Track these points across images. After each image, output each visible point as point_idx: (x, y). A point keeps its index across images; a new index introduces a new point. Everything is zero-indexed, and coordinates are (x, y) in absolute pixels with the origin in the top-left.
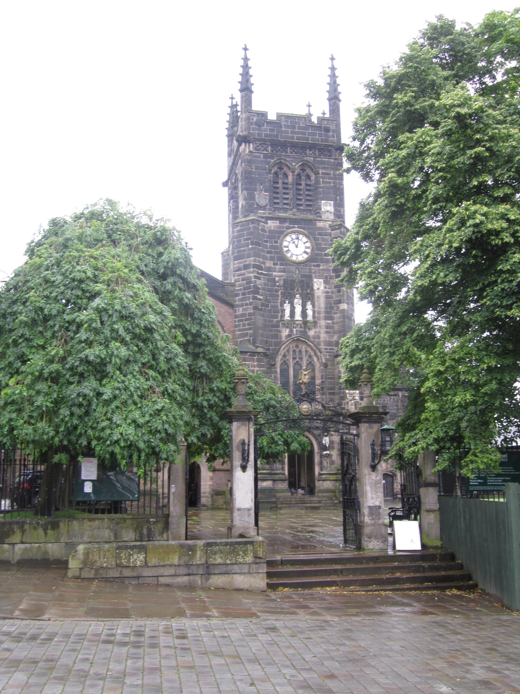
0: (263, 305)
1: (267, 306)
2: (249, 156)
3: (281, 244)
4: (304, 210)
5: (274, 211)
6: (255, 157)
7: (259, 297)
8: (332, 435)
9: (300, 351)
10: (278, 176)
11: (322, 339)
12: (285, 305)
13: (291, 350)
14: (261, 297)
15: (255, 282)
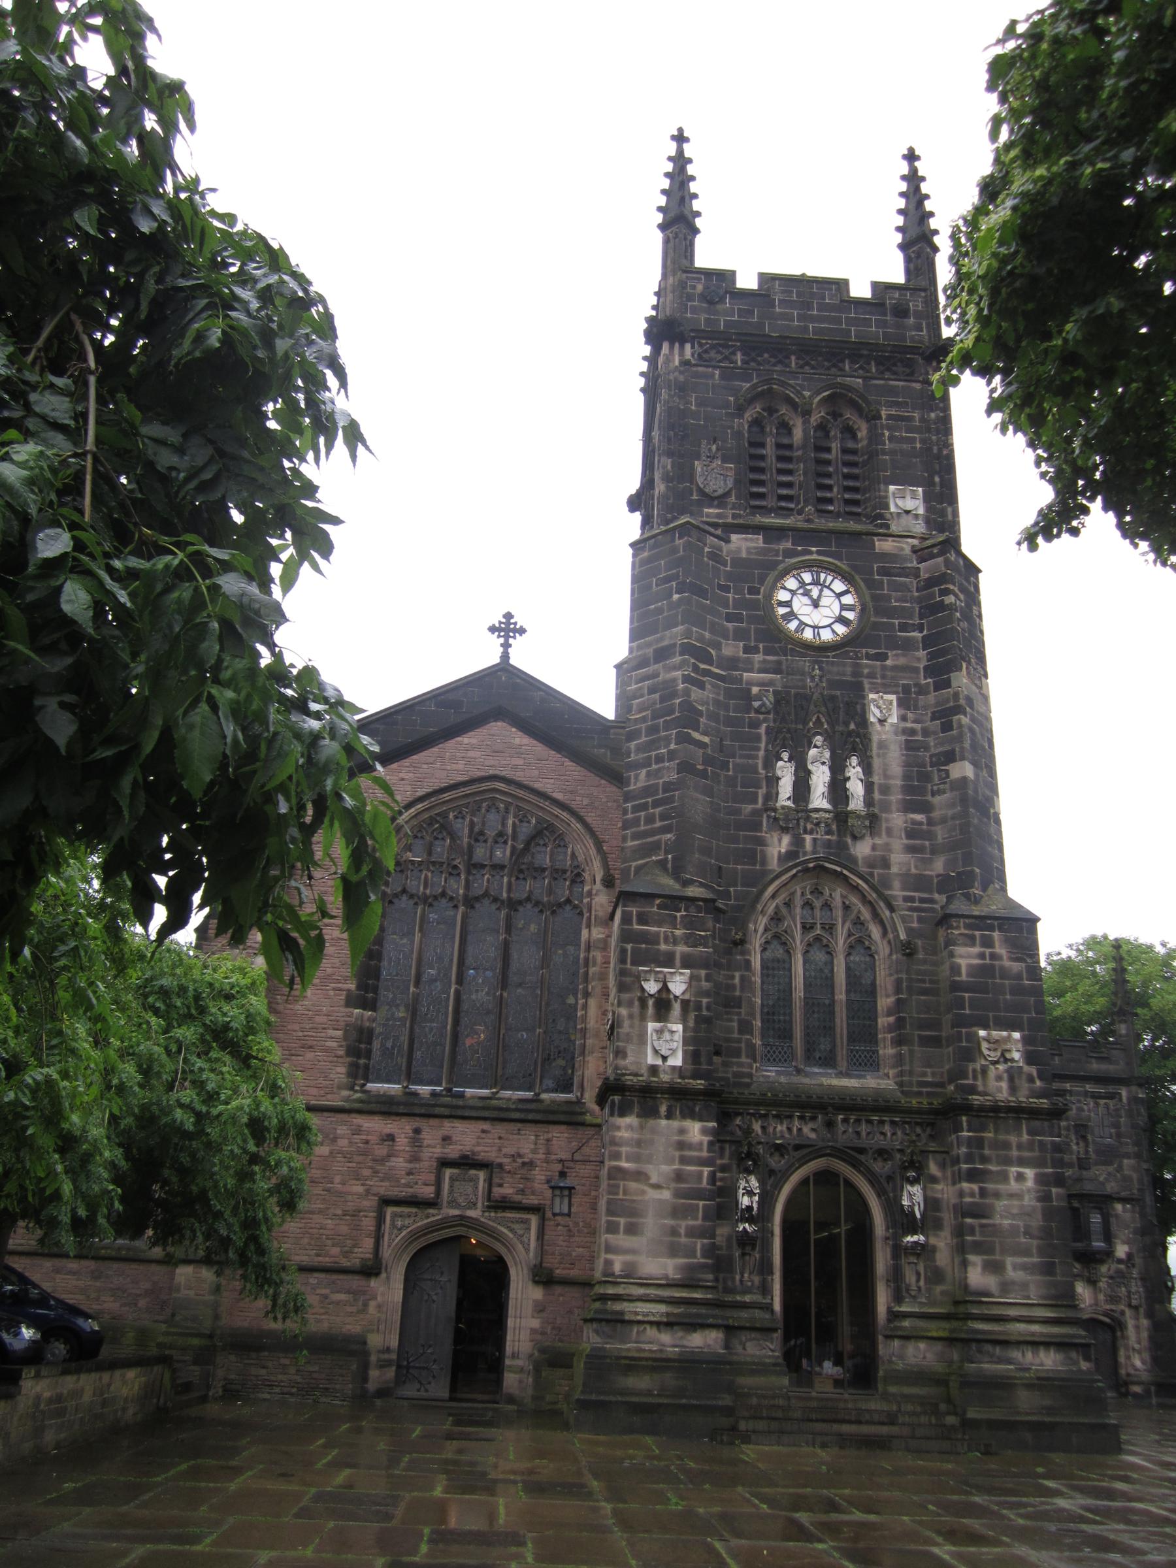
0: (708, 761)
1: (725, 766)
2: (681, 373)
3: (770, 596)
5: (753, 514)
6: (697, 375)
8: (934, 1180)
9: (827, 906)
11: (894, 870)
12: (780, 764)
13: (798, 901)
14: (706, 739)
15: (687, 692)
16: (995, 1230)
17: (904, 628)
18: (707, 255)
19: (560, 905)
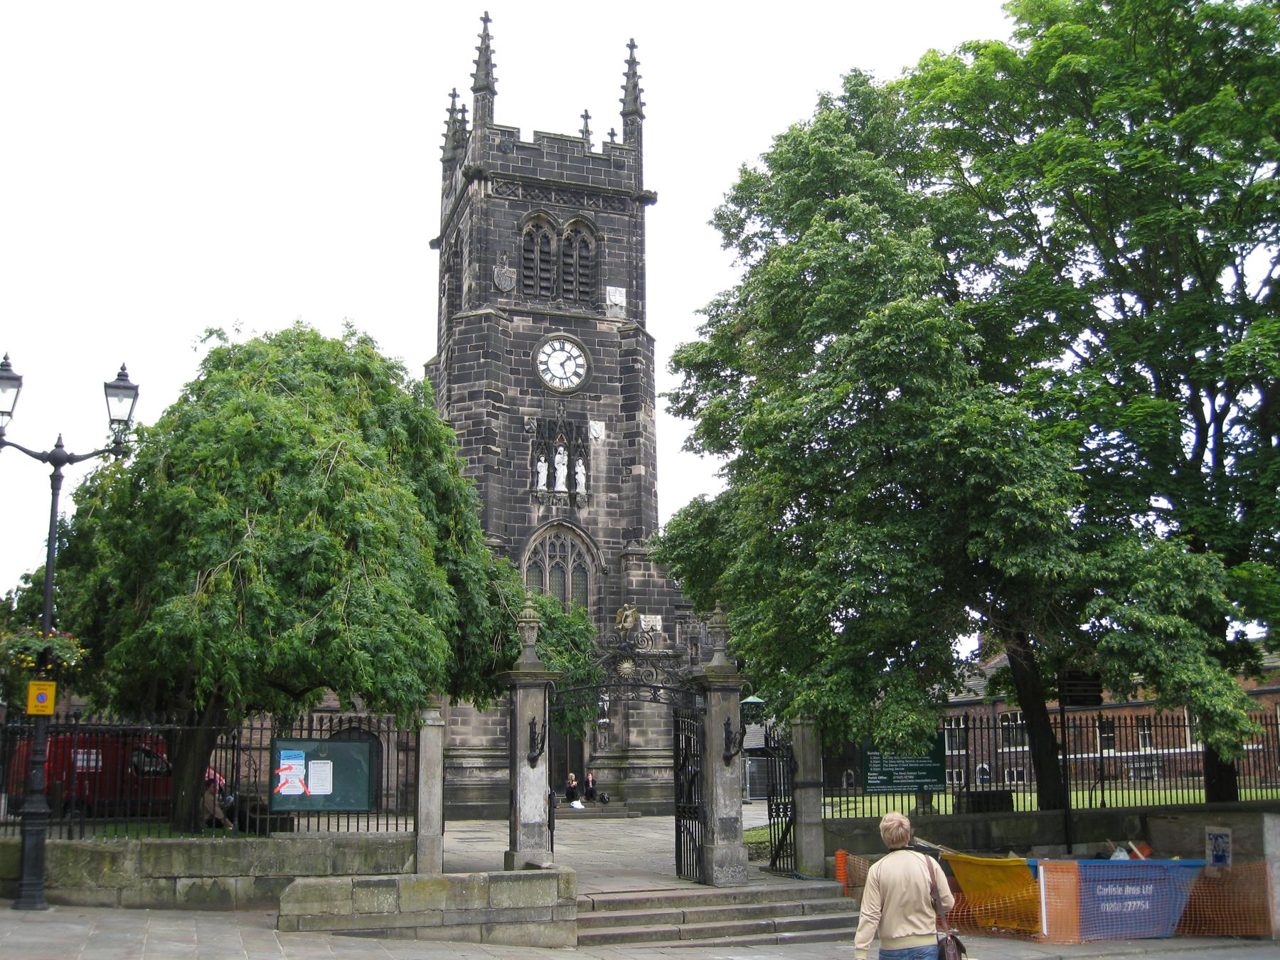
1: (509, 465)
3: (535, 359)
4: (575, 301)
5: (525, 300)
6: (494, 205)
7: (494, 448)
9: (562, 545)
10: (532, 240)
11: (600, 526)
12: (539, 463)
13: (548, 543)
14: (499, 450)
16: (644, 715)
17: (611, 380)
18: (502, 117)
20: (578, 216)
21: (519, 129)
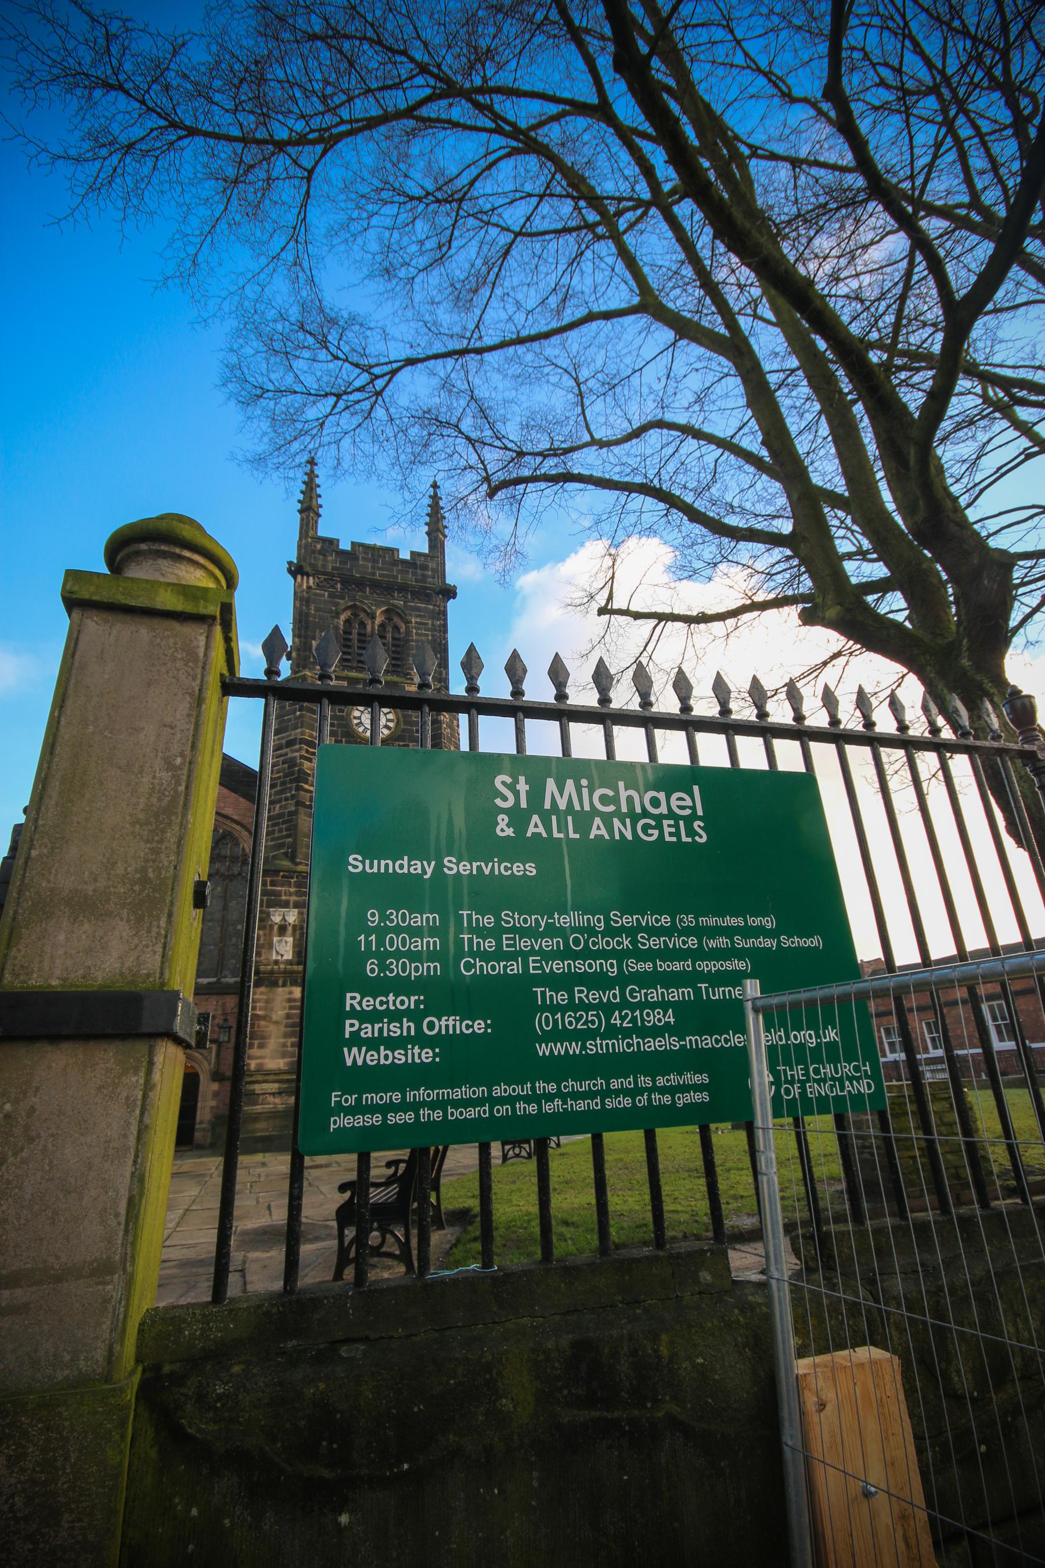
5: (343, 670)
6: (316, 594)
7: (306, 787)
18: (324, 530)
19: (234, 876)
20: (389, 604)
21: (338, 540)
